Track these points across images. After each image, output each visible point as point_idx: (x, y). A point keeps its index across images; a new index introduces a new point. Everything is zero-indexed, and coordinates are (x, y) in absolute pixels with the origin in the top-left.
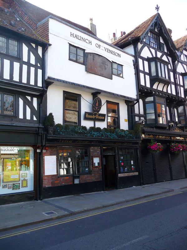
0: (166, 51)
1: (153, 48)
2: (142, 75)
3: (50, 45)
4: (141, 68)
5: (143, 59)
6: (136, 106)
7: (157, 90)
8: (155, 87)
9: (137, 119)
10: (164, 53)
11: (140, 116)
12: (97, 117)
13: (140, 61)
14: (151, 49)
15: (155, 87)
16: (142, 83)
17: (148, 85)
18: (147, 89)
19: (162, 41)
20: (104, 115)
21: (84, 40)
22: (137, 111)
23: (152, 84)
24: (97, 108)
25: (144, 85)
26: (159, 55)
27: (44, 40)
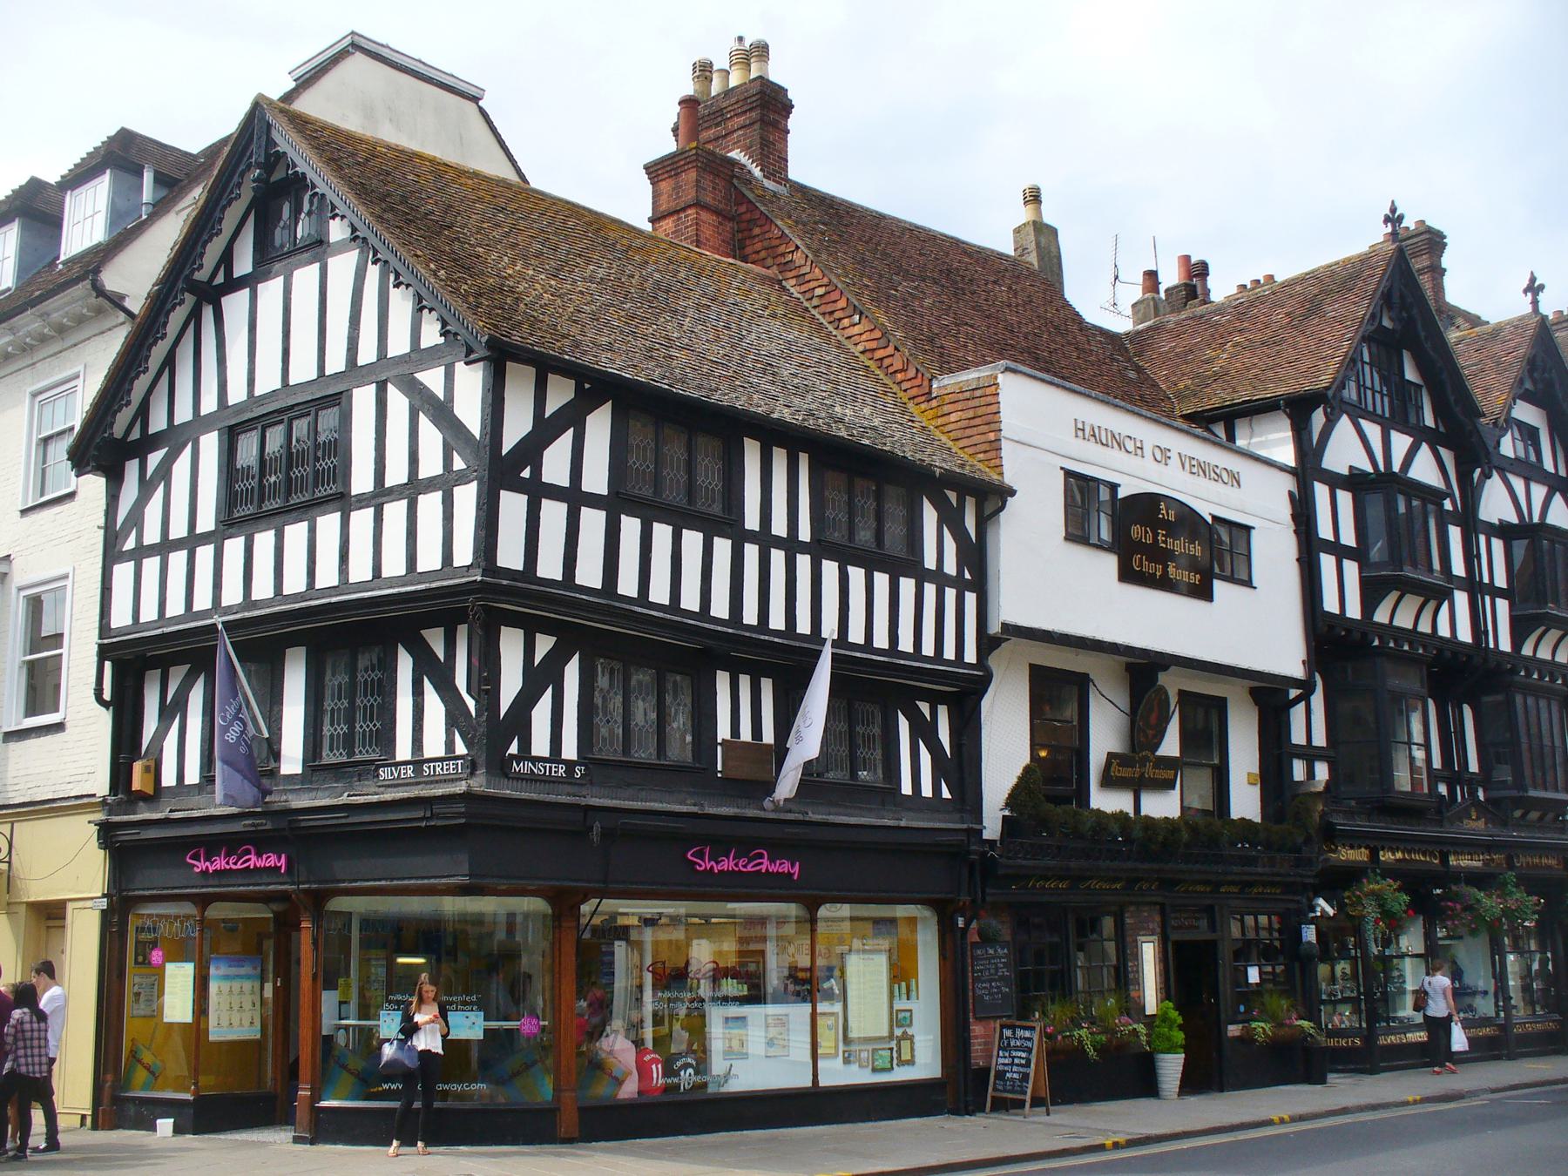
0: (1429, 421)
1: (1373, 417)
2: (1327, 562)
3: (1012, 493)
4: (1325, 531)
5: (1335, 482)
6: (1297, 714)
7: (1390, 630)
8: (1381, 616)
9: (1299, 770)
10: (1420, 435)
11: (1310, 754)
12: (1150, 771)
13: (1321, 492)
14: (1363, 422)
15: (1381, 616)
16: (1330, 604)
17: (1354, 611)
18: (1348, 631)
19: (1411, 374)
20: (1168, 762)
21: (1118, 442)
22: (1298, 737)
23: (1369, 605)
24: (1150, 732)
25: (1336, 611)
26: (1401, 443)
27: (977, 467)
